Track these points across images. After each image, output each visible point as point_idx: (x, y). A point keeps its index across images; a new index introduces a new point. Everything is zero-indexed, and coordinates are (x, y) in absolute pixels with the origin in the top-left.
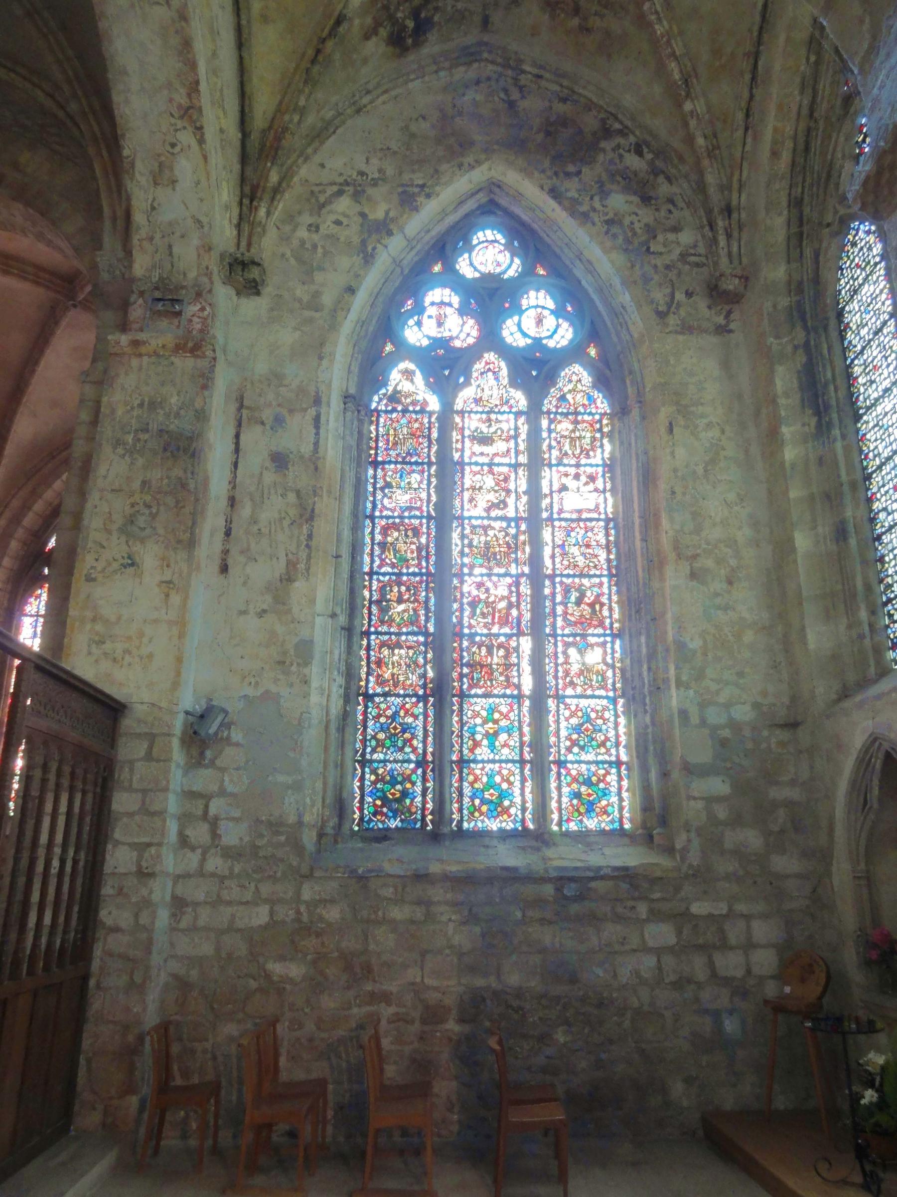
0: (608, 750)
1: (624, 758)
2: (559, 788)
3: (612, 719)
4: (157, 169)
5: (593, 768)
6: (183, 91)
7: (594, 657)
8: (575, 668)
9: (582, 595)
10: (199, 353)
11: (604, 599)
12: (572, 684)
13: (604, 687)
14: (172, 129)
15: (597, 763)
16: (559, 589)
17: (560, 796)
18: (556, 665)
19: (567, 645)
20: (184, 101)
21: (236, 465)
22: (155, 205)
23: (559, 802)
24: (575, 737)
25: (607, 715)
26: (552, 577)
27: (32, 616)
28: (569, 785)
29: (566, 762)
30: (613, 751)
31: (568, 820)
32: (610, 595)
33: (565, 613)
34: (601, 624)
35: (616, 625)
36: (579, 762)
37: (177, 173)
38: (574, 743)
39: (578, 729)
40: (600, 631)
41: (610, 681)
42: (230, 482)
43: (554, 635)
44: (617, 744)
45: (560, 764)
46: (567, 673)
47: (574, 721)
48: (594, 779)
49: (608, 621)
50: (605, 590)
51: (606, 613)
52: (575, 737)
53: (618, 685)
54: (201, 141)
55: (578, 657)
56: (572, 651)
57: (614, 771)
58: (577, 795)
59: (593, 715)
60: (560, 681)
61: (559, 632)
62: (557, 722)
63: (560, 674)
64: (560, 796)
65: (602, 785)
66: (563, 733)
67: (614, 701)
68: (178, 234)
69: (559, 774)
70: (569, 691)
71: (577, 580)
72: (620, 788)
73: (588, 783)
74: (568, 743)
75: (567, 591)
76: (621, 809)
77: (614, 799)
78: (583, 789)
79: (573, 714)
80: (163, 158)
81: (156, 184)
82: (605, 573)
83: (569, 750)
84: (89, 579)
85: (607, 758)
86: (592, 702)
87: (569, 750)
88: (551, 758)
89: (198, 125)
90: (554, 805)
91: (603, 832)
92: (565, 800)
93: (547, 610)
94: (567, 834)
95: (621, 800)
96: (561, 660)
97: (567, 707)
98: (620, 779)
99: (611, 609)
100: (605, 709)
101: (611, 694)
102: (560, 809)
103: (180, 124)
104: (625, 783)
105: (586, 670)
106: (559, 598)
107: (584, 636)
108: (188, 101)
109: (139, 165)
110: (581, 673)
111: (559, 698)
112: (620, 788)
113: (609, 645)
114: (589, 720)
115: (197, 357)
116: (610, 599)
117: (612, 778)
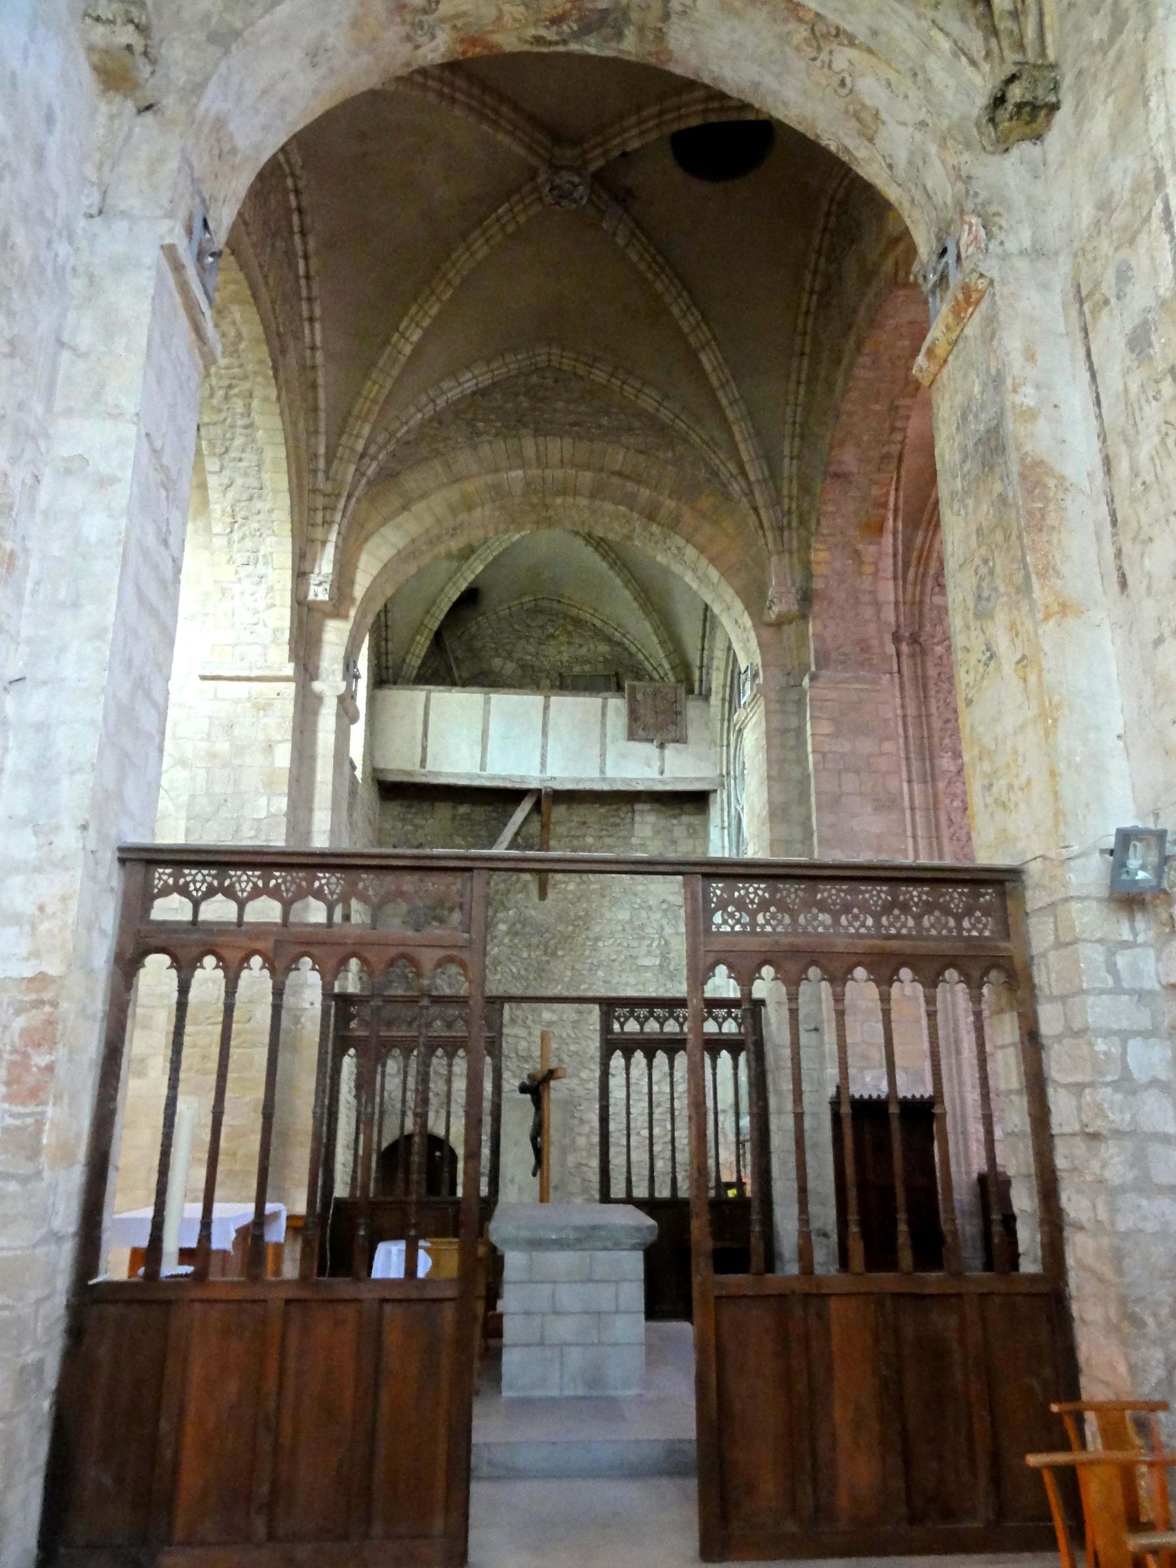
4: (857, 125)
6: (792, 25)
10: (975, 296)
14: (826, 70)
20: (803, 32)
21: (1098, 402)
22: (888, 161)
37: (868, 102)
42: (1099, 436)
54: (852, 43)
68: (920, 164)
80: (851, 108)
81: (871, 140)
89: (834, 32)
103: (824, 56)
108: (805, 26)
109: (850, 143)
115: (978, 302)
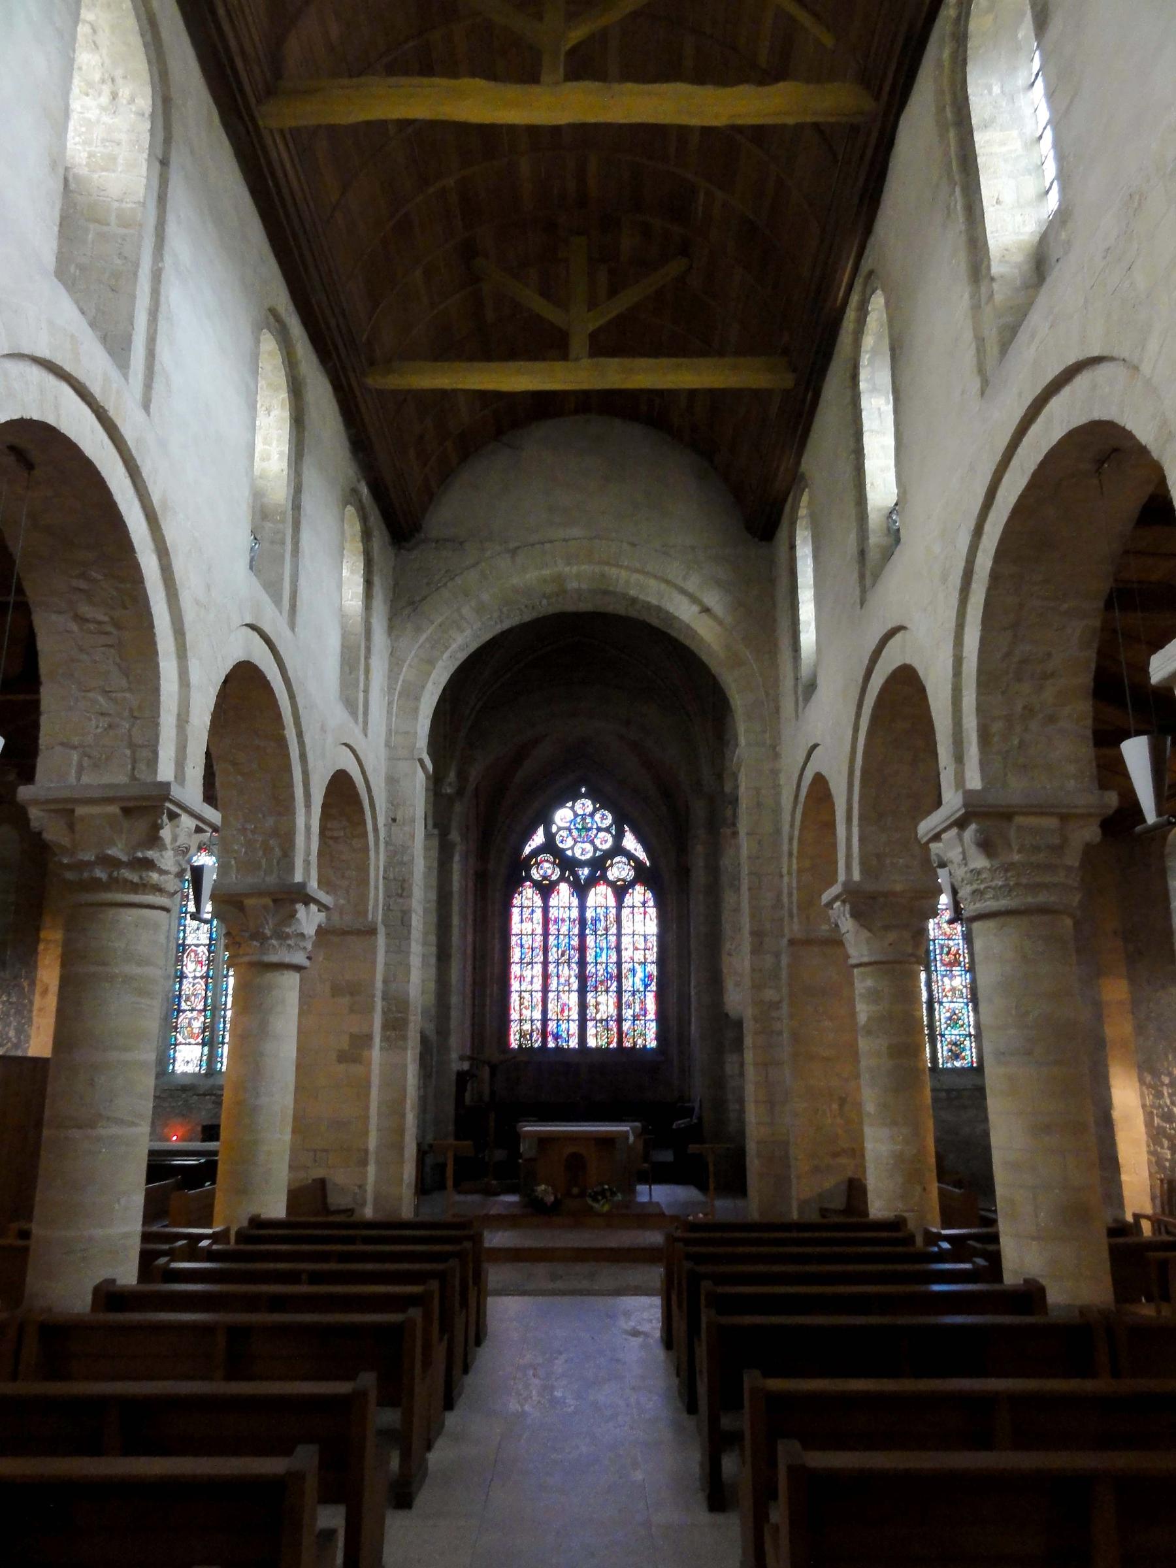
0: (965, 1030)
1: (973, 1032)
2: (942, 1047)
3: (966, 1013)
5: (958, 1037)
7: (957, 982)
8: (948, 987)
9: (950, 950)
11: (961, 952)
12: (946, 996)
13: (962, 997)
15: (960, 1035)
16: (937, 947)
17: (942, 1051)
18: (938, 987)
19: (944, 976)
23: (943, 1055)
24: (949, 1022)
25: (963, 1011)
26: (934, 940)
27: (517, 907)
28: (947, 1045)
29: (944, 1035)
30: (967, 1029)
31: (947, 1063)
32: (964, 949)
33: (941, 960)
34: (959, 965)
35: (967, 965)
36: (951, 1035)
38: (949, 1025)
39: (950, 1018)
40: (959, 968)
41: (965, 995)
43: (936, 971)
44: (969, 1026)
45: (942, 1036)
46: (944, 990)
47: (948, 1014)
48: (958, 1043)
49: (963, 963)
50: (961, 947)
51: (961, 959)
52: (949, 1022)
53: (969, 996)
55: (949, 981)
56: (946, 979)
57: (968, 1039)
58: (950, 1050)
59: (957, 1012)
60: (940, 994)
61: (938, 969)
62: (940, 1015)
63: (940, 991)
64: (942, 1051)
65: (962, 1046)
66: (943, 1021)
67: (967, 1005)
69: (942, 1041)
70: (945, 1000)
71: (946, 942)
72: (971, 1047)
73: (955, 1044)
74: (945, 1026)
75: (942, 947)
76: (972, 1057)
77: (968, 1052)
78: (953, 1047)
79: (948, 1011)
82: (961, 937)
83: (946, 1029)
84: (730, 955)
85: (964, 1032)
86: (956, 1005)
87: (946, 1029)
88: (937, 1033)
90: (940, 1055)
91: (963, 1068)
92: (945, 1053)
93: (932, 958)
94: (947, 1069)
95: (972, 1053)
96: (940, 984)
97: (944, 1007)
98: (971, 1043)
99: (964, 957)
100: (962, 1008)
101: (965, 1001)
102: (943, 1057)
104: (973, 1045)
105: (953, 989)
106: (938, 952)
107: (951, 971)
110: (950, 990)
111: (941, 1003)
112: (971, 1047)
113: (963, 976)
114: (955, 1014)
116: (964, 953)
117: (967, 1043)
